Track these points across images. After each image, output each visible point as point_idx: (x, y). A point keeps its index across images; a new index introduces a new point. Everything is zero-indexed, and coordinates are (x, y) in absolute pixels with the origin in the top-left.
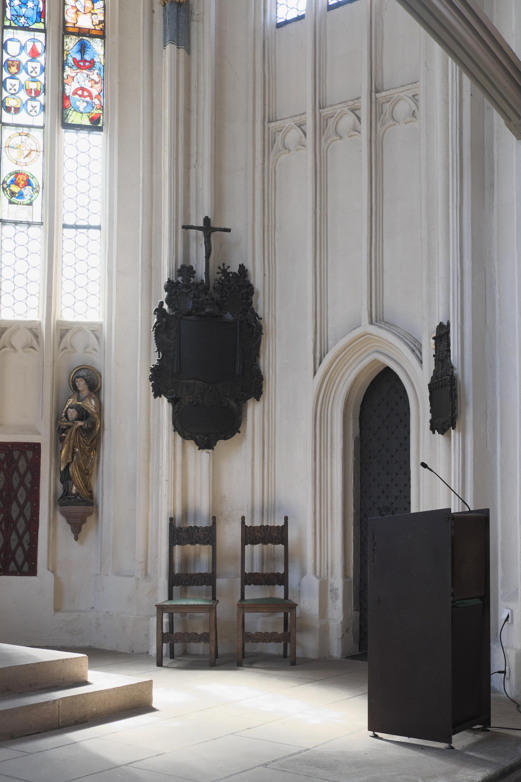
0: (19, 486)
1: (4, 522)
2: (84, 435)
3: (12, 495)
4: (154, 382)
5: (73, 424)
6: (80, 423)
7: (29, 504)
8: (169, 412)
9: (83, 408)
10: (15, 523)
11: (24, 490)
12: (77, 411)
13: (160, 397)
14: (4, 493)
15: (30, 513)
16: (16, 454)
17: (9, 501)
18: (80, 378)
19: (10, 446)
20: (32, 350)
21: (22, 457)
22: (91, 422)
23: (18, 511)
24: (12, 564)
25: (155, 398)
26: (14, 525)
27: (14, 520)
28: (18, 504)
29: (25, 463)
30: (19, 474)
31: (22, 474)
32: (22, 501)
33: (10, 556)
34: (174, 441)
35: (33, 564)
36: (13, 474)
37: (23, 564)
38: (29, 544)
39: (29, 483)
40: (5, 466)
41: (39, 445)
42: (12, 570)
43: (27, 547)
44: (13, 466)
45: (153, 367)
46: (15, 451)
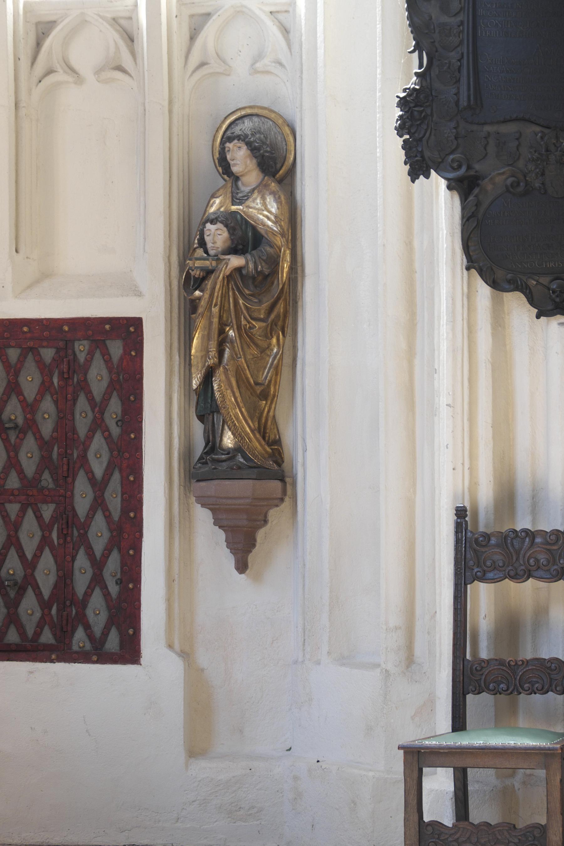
0: (92, 432)
1: (56, 526)
2: (247, 292)
3: (75, 455)
4: (408, 137)
5: (217, 264)
6: (236, 261)
7: (116, 477)
8: (452, 216)
9: (247, 222)
10: (85, 526)
11: (103, 440)
12: (229, 231)
13: (427, 176)
14: (56, 448)
15: (119, 499)
16: (81, 348)
17: (68, 470)
18: (236, 141)
19: (66, 328)
20: (119, 75)
21: (98, 355)
22: (265, 258)
23: (90, 496)
24: (80, 634)
25: (413, 181)
26: (81, 531)
27: (82, 520)
28: (89, 479)
29: (105, 372)
30: (91, 399)
31: (98, 398)
32: (98, 470)
33: (74, 612)
34: (470, 296)
35: (131, 631)
36: (77, 399)
37: (105, 633)
38: (119, 582)
39: (117, 423)
40: (55, 380)
41: (137, 323)
42: (80, 647)
43: (114, 589)
44: (75, 380)
45: (402, 95)
46: (80, 340)
